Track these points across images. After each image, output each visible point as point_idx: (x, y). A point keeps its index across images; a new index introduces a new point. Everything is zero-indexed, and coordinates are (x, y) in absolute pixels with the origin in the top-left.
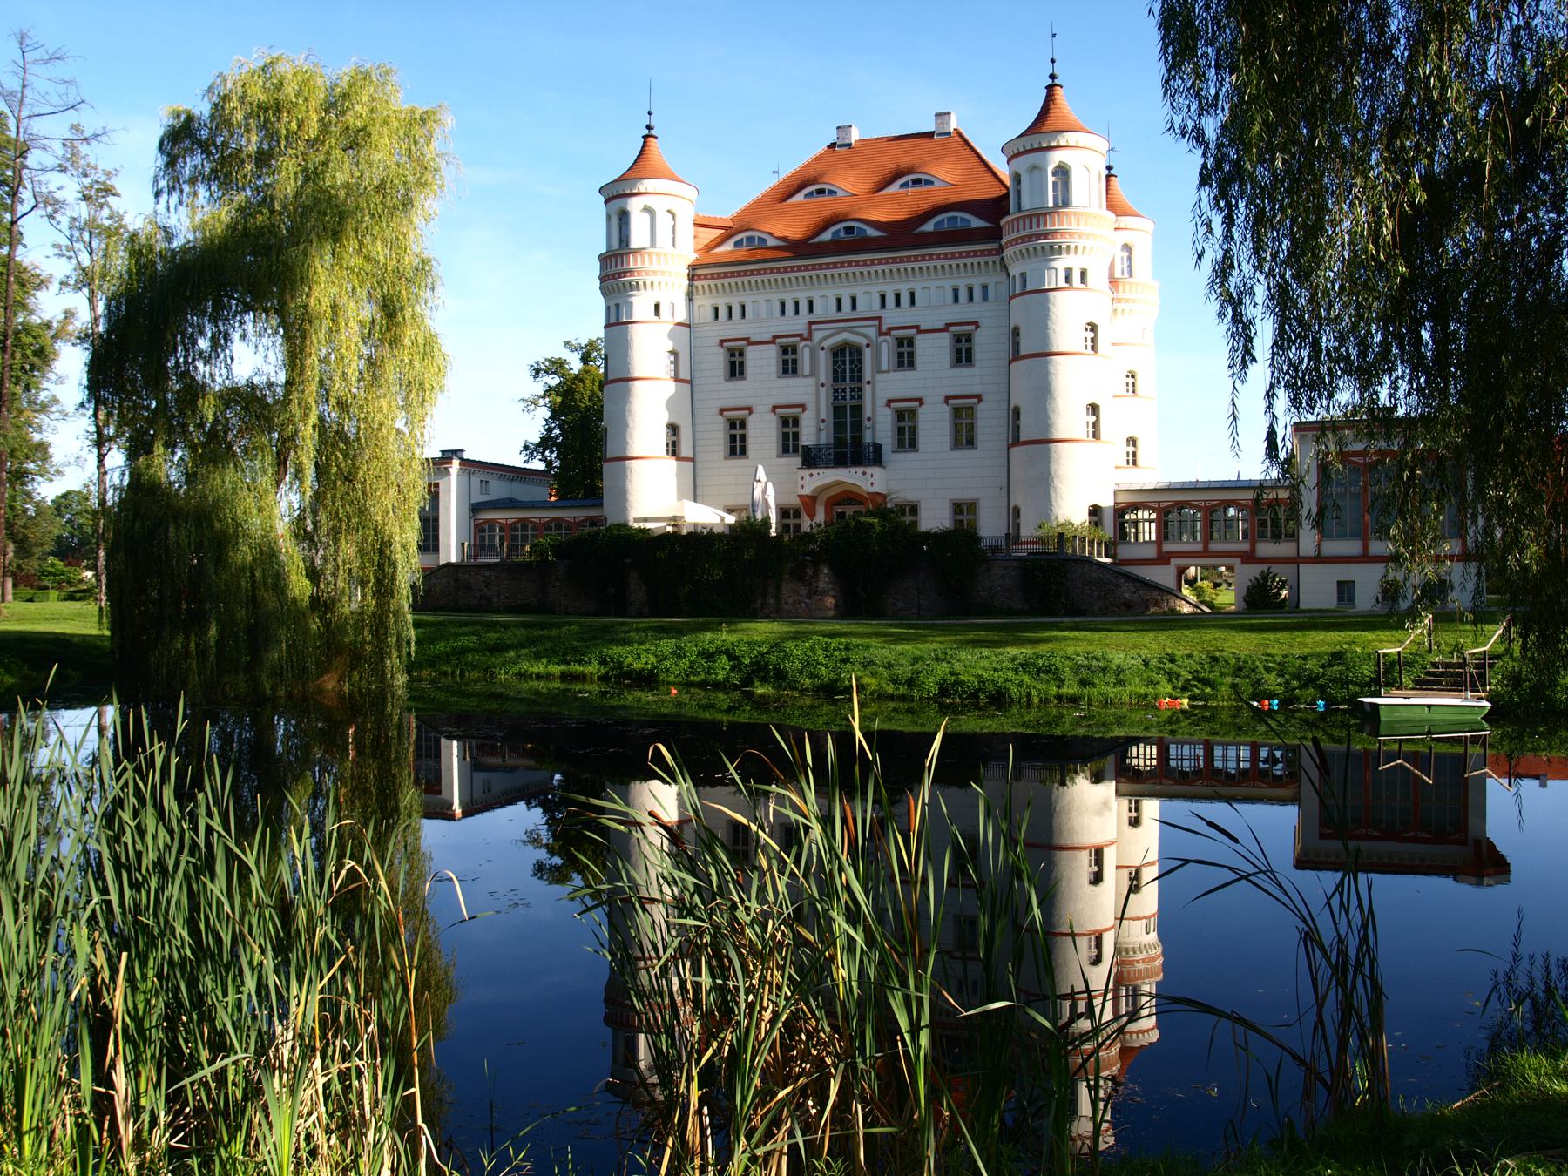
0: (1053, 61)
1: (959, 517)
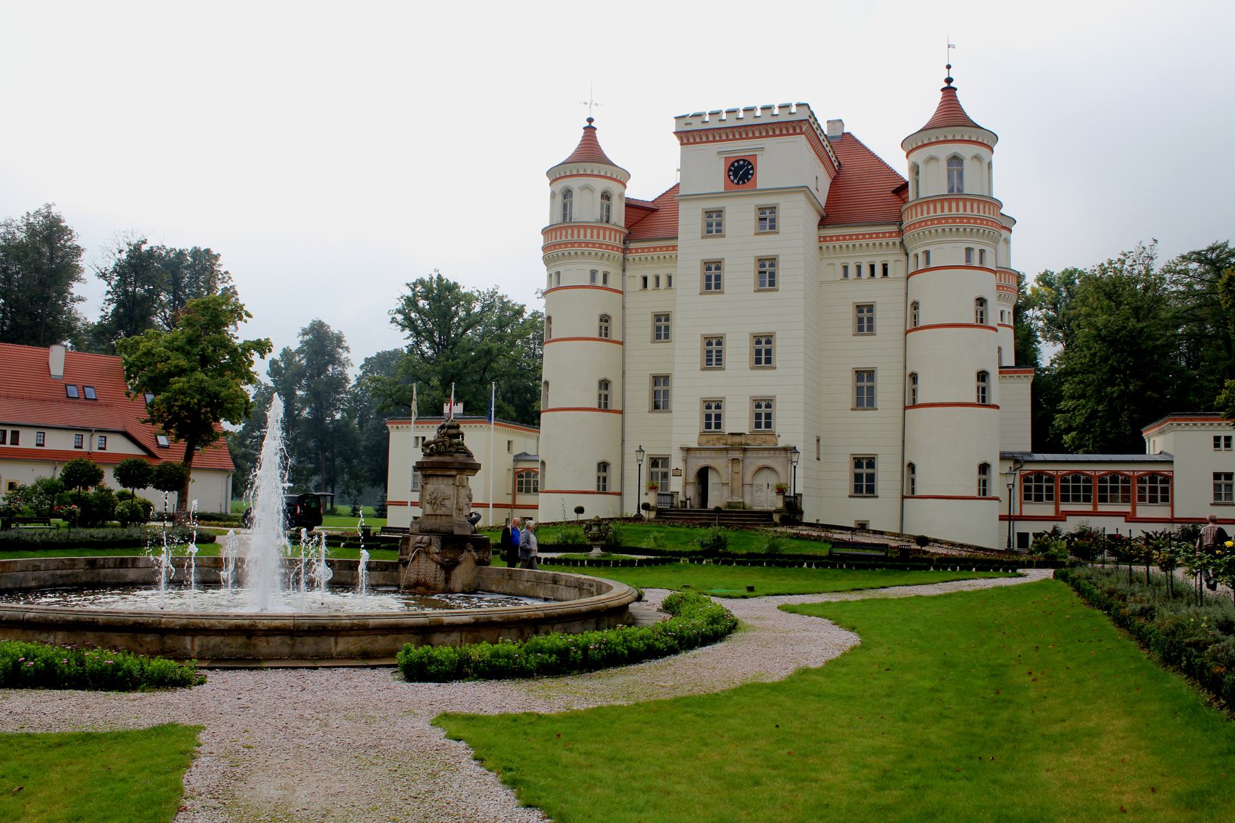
0: (949, 67)
1: (859, 471)
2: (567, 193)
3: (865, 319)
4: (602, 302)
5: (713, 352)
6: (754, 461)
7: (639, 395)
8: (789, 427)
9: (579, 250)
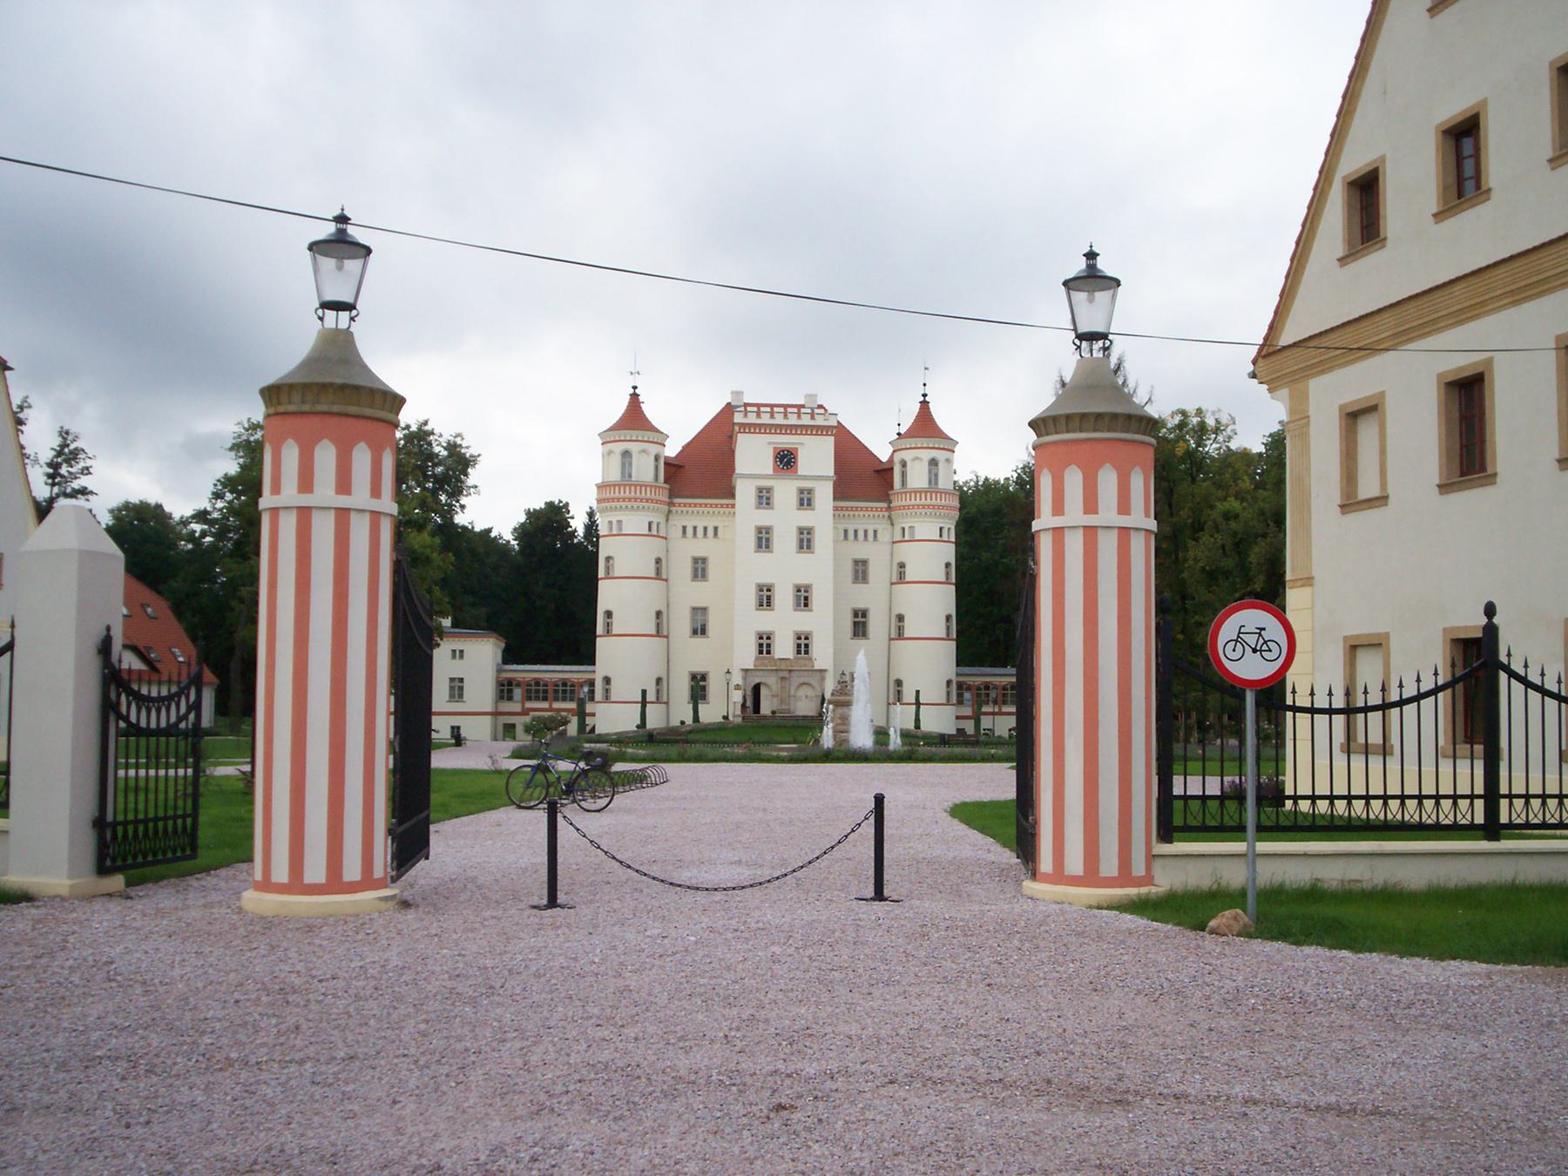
2: (626, 454)
3: (860, 570)
4: (653, 547)
5: (765, 598)
6: (796, 680)
7: (680, 624)
8: (822, 655)
9: (635, 505)
